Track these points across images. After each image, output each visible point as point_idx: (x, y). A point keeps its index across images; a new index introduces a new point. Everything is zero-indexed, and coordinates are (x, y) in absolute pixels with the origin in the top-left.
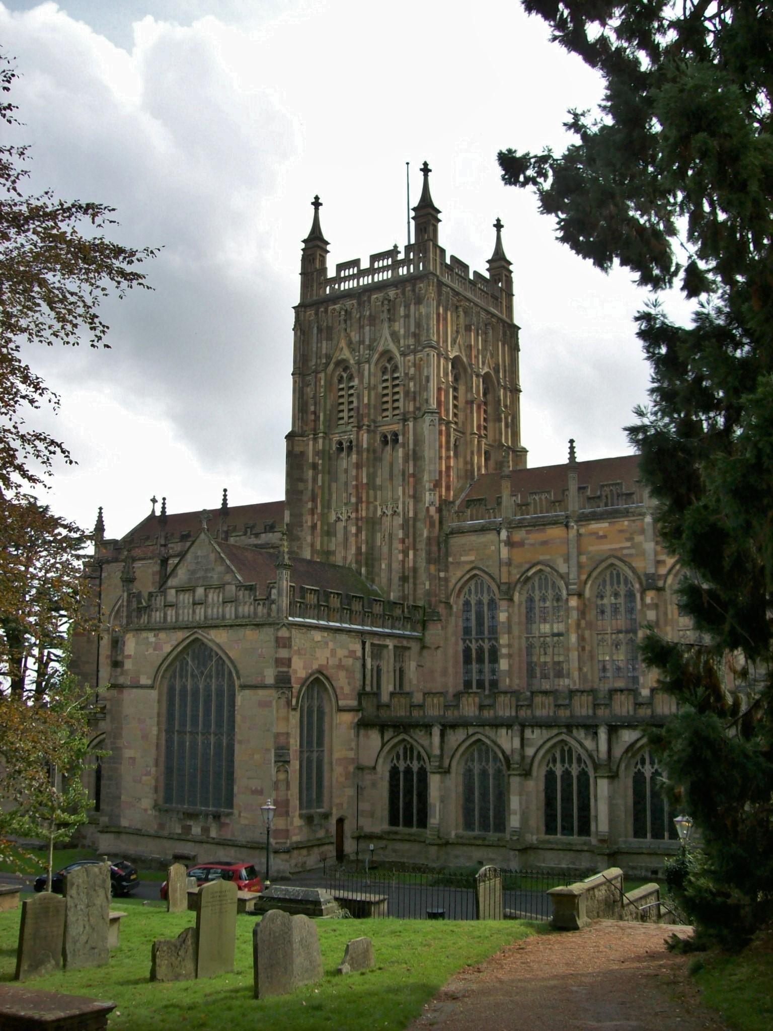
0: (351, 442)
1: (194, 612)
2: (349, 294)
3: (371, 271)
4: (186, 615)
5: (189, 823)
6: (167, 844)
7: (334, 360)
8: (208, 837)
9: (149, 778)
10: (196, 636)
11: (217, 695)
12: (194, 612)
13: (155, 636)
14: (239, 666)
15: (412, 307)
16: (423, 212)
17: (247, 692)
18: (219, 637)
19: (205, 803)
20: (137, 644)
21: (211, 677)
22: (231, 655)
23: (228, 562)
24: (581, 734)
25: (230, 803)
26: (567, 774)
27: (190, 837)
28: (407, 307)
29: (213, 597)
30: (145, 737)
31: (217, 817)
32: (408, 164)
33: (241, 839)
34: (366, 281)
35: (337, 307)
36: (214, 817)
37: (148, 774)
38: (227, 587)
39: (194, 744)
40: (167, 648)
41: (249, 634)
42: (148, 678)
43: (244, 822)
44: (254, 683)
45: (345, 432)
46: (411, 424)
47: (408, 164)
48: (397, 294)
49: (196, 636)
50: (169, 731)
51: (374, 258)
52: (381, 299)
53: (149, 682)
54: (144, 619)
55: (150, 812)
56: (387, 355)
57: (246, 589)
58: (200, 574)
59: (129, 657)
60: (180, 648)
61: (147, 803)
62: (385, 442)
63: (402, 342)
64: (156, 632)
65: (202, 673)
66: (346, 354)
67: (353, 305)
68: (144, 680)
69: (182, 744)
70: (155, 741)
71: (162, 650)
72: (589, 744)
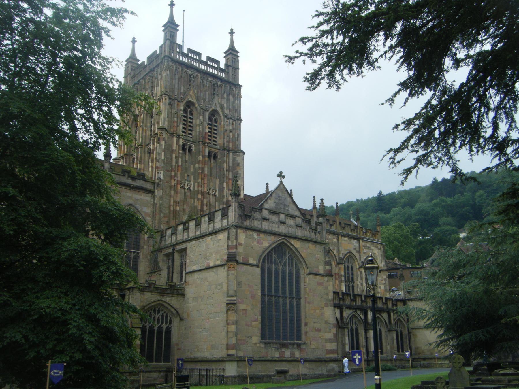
0: (190, 147)
1: (279, 227)
2: (198, 70)
3: (203, 63)
4: (276, 228)
5: (284, 350)
6: (269, 365)
7: (187, 99)
8: (295, 358)
9: (257, 323)
10: (283, 240)
11: (289, 276)
12: (279, 227)
13: (257, 235)
14: (307, 262)
15: (231, 96)
16: (229, 53)
17: (311, 276)
18: (297, 244)
19: (278, 338)
20: (246, 237)
21: (285, 265)
22: (302, 255)
23: (262, 203)
24: (359, 312)
25: (299, 338)
26: (352, 328)
27: (285, 359)
28: (228, 96)
29: (290, 222)
30: (253, 297)
31: (299, 346)
32: (184, 11)
33: (312, 357)
34: (203, 67)
35: (189, 72)
36: (297, 345)
37: (256, 320)
38: (297, 219)
39: (277, 302)
40: (266, 244)
41: (311, 246)
42: (254, 260)
43: (313, 347)
44: (314, 272)
45: (189, 141)
46: (231, 154)
47: (184, 11)
48: (220, 85)
49: (283, 240)
50: (263, 295)
51: (209, 58)
52: (213, 83)
53: (255, 262)
54: (247, 223)
55: (258, 345)
56: (214, 113)
57: (306, 222)
58: (282, 206)
59: (241, 244)
60: (274, 246)
61: (256, 339)
62: (209, 156)
63: (225, 110)
64: (259, 233)
65: (280, 262)
66: (194, 100)
67: (197, 75)
68: (251, 261)
69: (270, 302)
70: (260, 299)
71: (262, 244)
72: (362, 317)
